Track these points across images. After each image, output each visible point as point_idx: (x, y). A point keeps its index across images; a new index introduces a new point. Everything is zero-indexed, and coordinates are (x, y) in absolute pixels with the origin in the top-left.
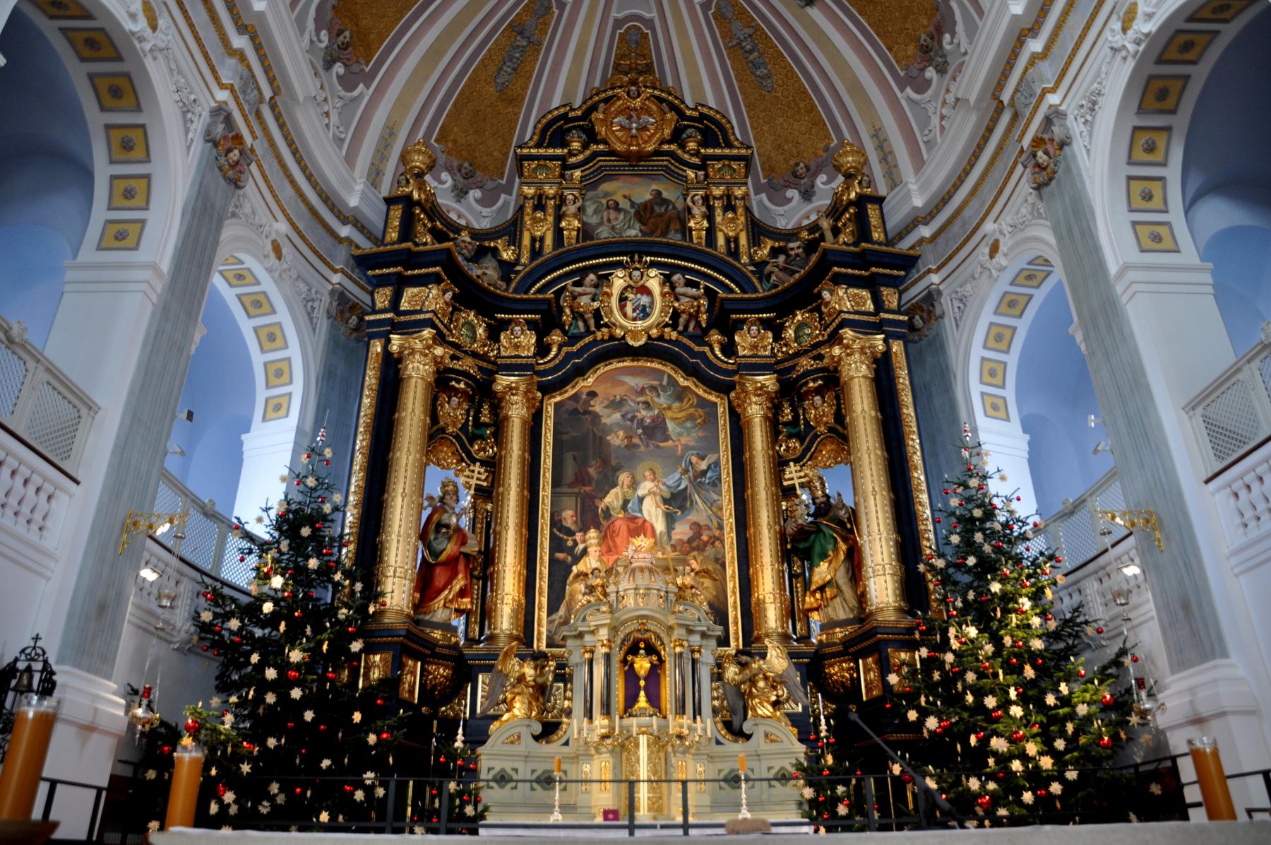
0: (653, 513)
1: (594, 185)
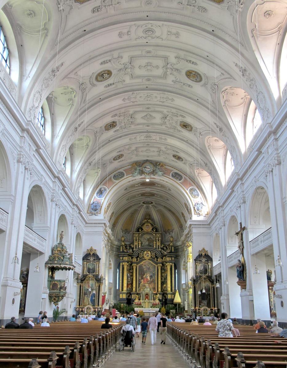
0: (149, 278)
1: (142, 236)
